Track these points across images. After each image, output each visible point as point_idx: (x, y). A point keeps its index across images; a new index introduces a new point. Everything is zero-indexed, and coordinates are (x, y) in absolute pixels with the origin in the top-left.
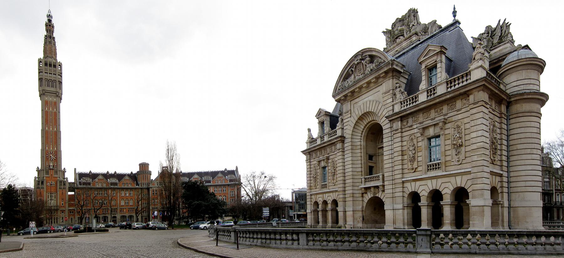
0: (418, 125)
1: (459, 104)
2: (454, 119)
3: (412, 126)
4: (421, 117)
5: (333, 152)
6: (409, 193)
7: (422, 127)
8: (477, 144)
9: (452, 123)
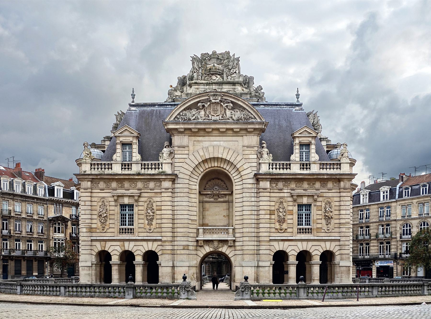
0: (289, 191)
1: (330, 185)
2: (325, 195)
3: (281, 189)
4: (293, 185)
5: (151, 189)
6: (276, 251)
7: (297, 194)
8: (346, 219)
9: (323, 198)
